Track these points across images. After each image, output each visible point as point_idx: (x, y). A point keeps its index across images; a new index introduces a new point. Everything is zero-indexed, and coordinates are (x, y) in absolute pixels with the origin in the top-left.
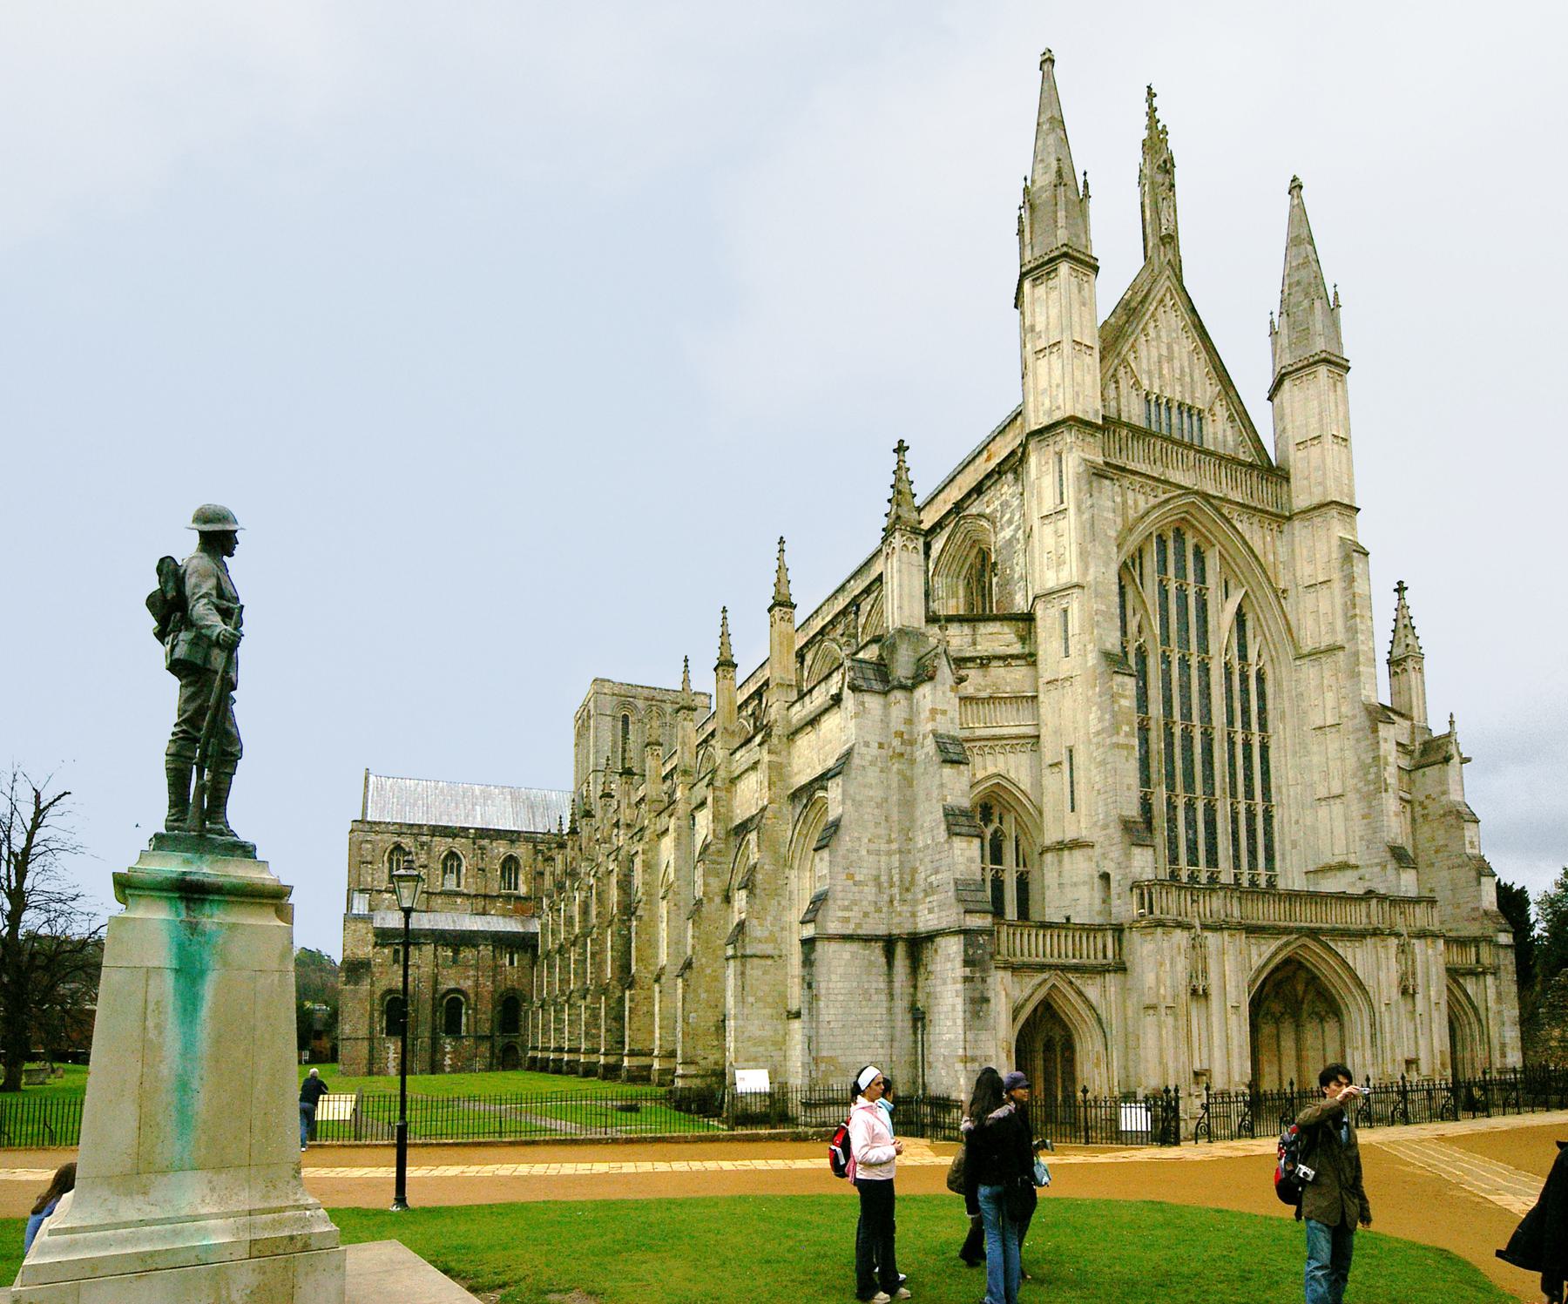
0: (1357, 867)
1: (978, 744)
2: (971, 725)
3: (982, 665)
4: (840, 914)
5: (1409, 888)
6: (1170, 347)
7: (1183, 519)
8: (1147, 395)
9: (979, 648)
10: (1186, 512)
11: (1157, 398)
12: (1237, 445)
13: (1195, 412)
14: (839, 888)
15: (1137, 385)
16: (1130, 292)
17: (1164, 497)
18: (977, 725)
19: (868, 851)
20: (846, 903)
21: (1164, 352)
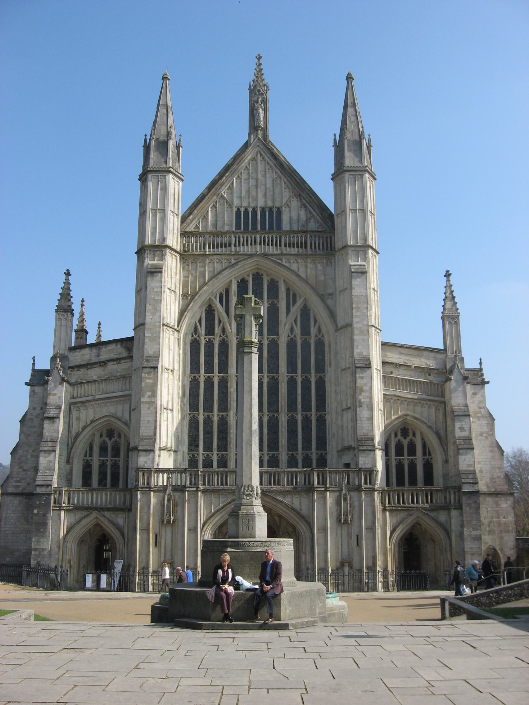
0: (354, 449)
1: (98, 402)
2: (93, 394)
3: (100, 365)
4: (14, 484)
5: (367, 462)
6: (257, 180)
7: (258, 268)
8: (238, 209)
9: (101, 357)
10: (257, 265)
11: (246, 209)
12: (308, 220)
13: (275, 210)
14: (15, 473)
15: (230, 205)
16: (232, 160)
17: (233, 261)
18: (97, 394)
19: (32, 456)
20: (18, 479)
21: (252, 182)
